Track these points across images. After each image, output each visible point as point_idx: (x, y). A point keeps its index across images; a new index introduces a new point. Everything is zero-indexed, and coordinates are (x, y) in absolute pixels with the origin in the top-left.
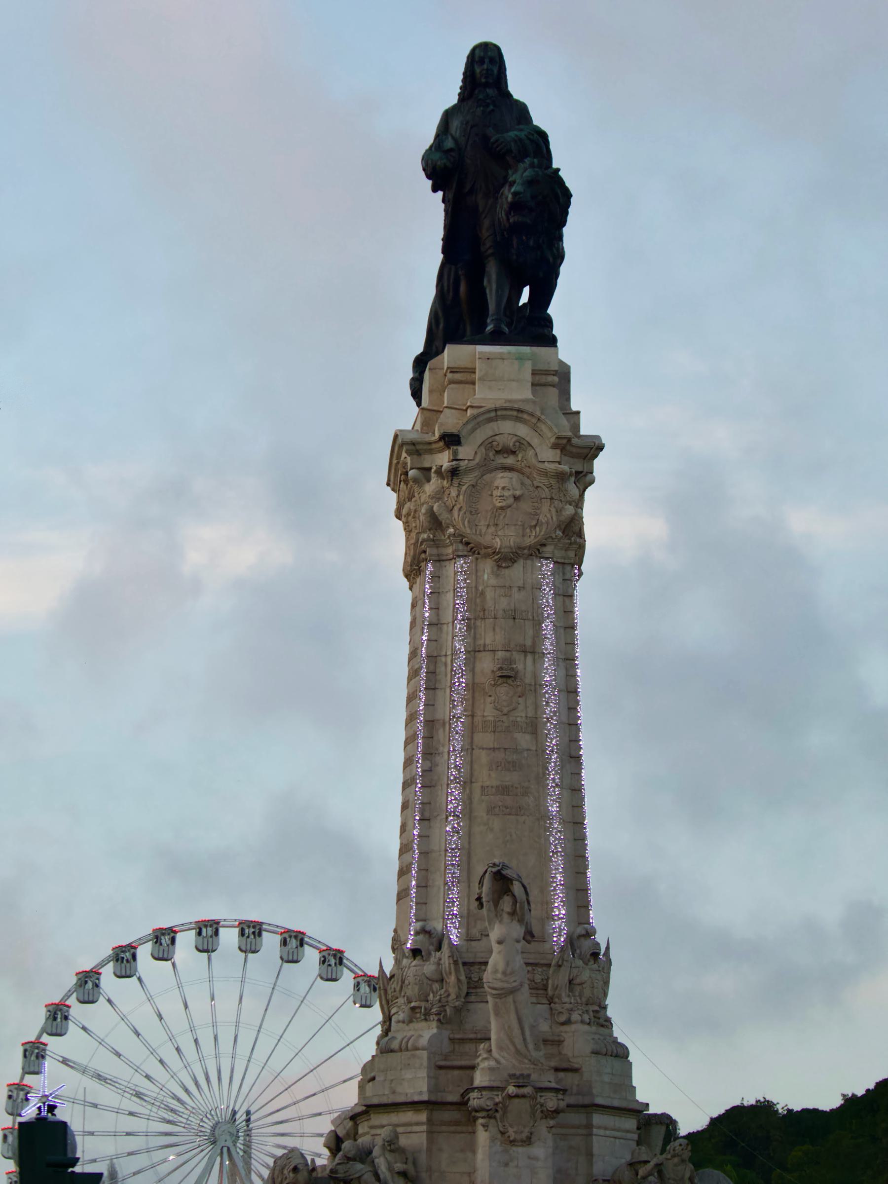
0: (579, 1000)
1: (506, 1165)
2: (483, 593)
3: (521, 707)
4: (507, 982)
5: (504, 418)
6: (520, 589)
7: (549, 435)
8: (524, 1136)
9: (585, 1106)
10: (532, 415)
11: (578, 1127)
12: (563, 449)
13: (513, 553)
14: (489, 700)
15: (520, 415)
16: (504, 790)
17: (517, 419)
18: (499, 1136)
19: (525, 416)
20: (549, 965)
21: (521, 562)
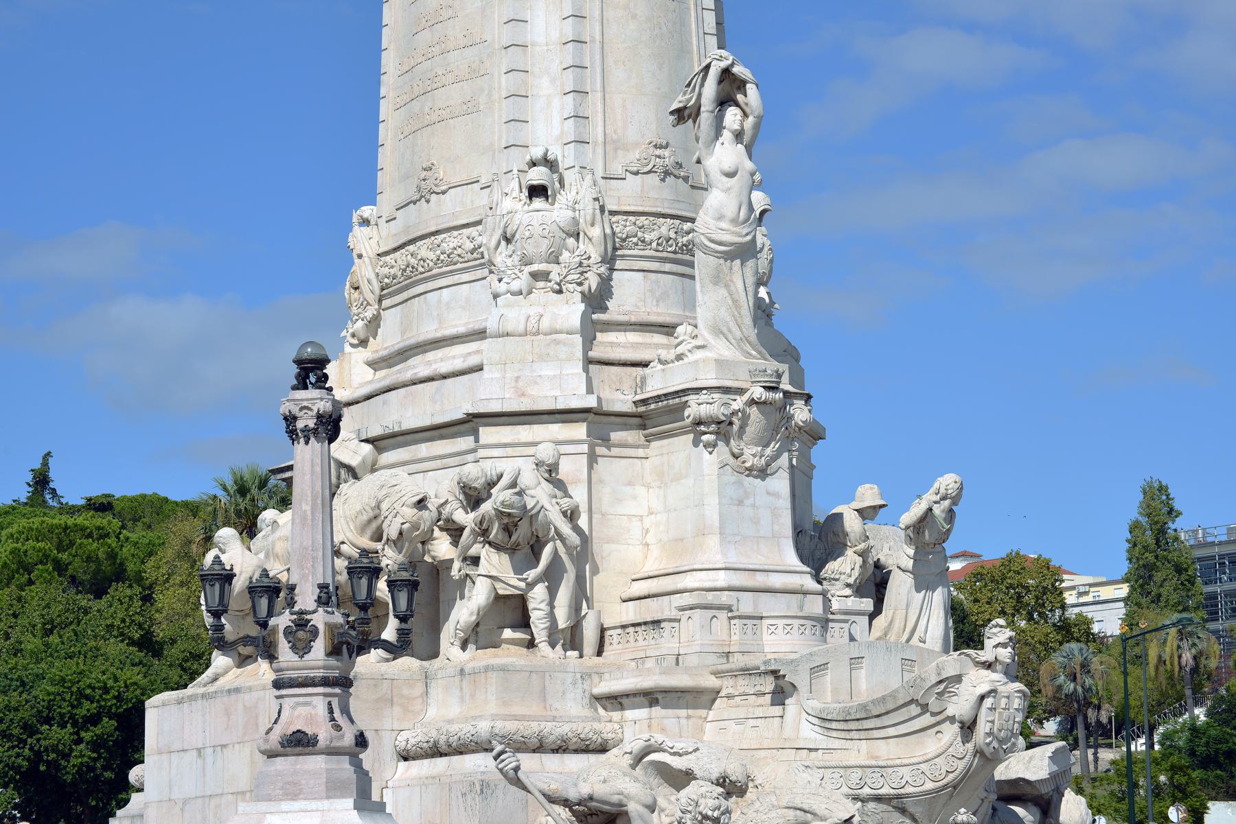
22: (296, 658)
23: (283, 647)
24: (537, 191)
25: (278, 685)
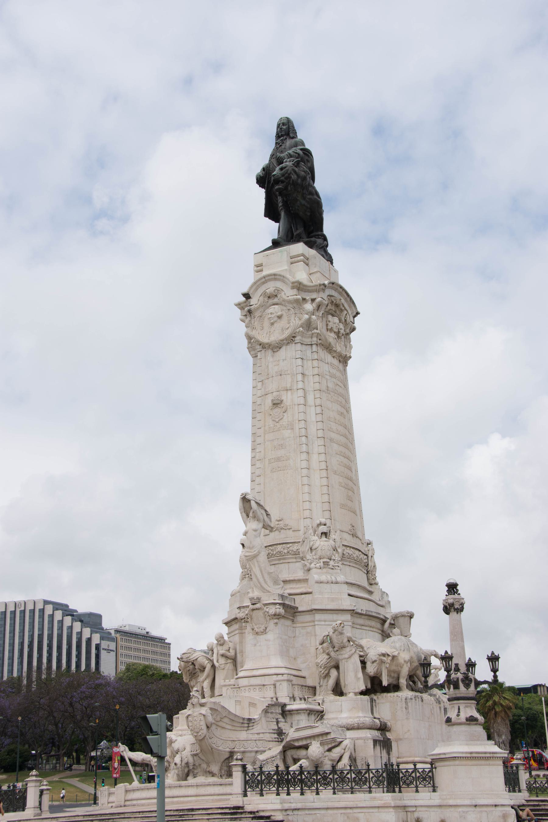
0: (315, 557)
1: (255, 645)
2: (268, 367)
3: (285, 418)
4: (251, 552)
5: (270, 280)
6: (283, 360)
7: (289, 283)
8: (261, 630)
9: (311, 610)
10: (280, 275)
11: (310, 622)
12: (299, 289)
13: (277, 343)
14: (271, 417)
15: (276, 277)
16: (278, 459)
17: (275, 279)
18: (251, 631)
19: (278, 277)
20: (299, 542)
21: (284, 347)
22: (466, 689)
23: (461, 685)
24: (325, 534)
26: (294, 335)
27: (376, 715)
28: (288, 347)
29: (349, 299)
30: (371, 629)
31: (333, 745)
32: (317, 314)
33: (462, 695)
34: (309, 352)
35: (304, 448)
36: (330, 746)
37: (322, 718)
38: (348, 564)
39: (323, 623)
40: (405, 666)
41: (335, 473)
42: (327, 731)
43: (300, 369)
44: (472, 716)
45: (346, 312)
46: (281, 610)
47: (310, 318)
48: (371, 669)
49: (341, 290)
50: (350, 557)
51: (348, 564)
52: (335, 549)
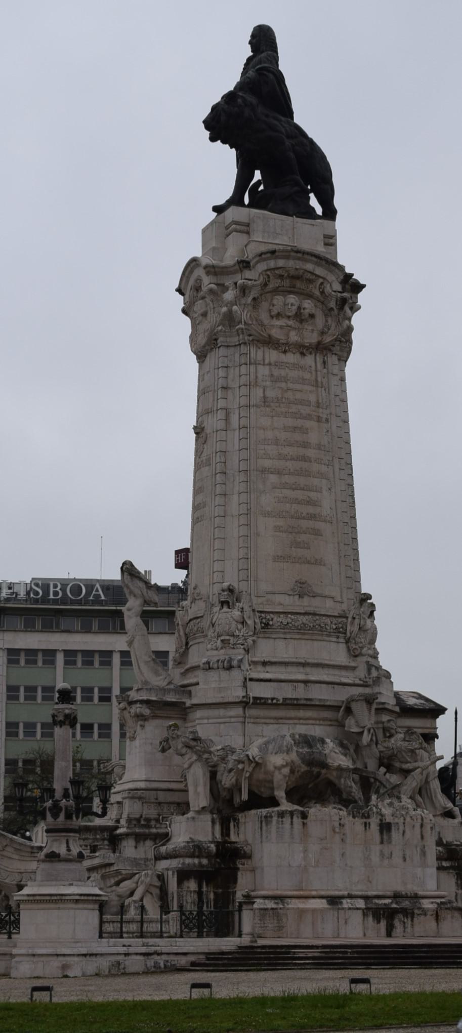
12: (215, 274)
23: (48, 814)
25: (47, 831)
26: (214, 337)
27: (233, 838)
28: (213, 353)
29: (324, 263)
30: (301, 721)
31: (120, 877)
32: (243, 301)
33: (61, 827)
34: (237, 355)
35: (219, 489)
36: (117, 879)
37: (169, 840)
38: (282, 636)
39: (206, 721)
40: (277, 773)
41: (267, 514)
42: (107, 861)
43: (221, 382)
44: (53, 852)
45: (321, 280)
46: (147, 711)
47: (230, 311)
48: (227, 780)
49: (299, 255)
50: (285, 627)
51: (282, 636)
52: (243, 622)
